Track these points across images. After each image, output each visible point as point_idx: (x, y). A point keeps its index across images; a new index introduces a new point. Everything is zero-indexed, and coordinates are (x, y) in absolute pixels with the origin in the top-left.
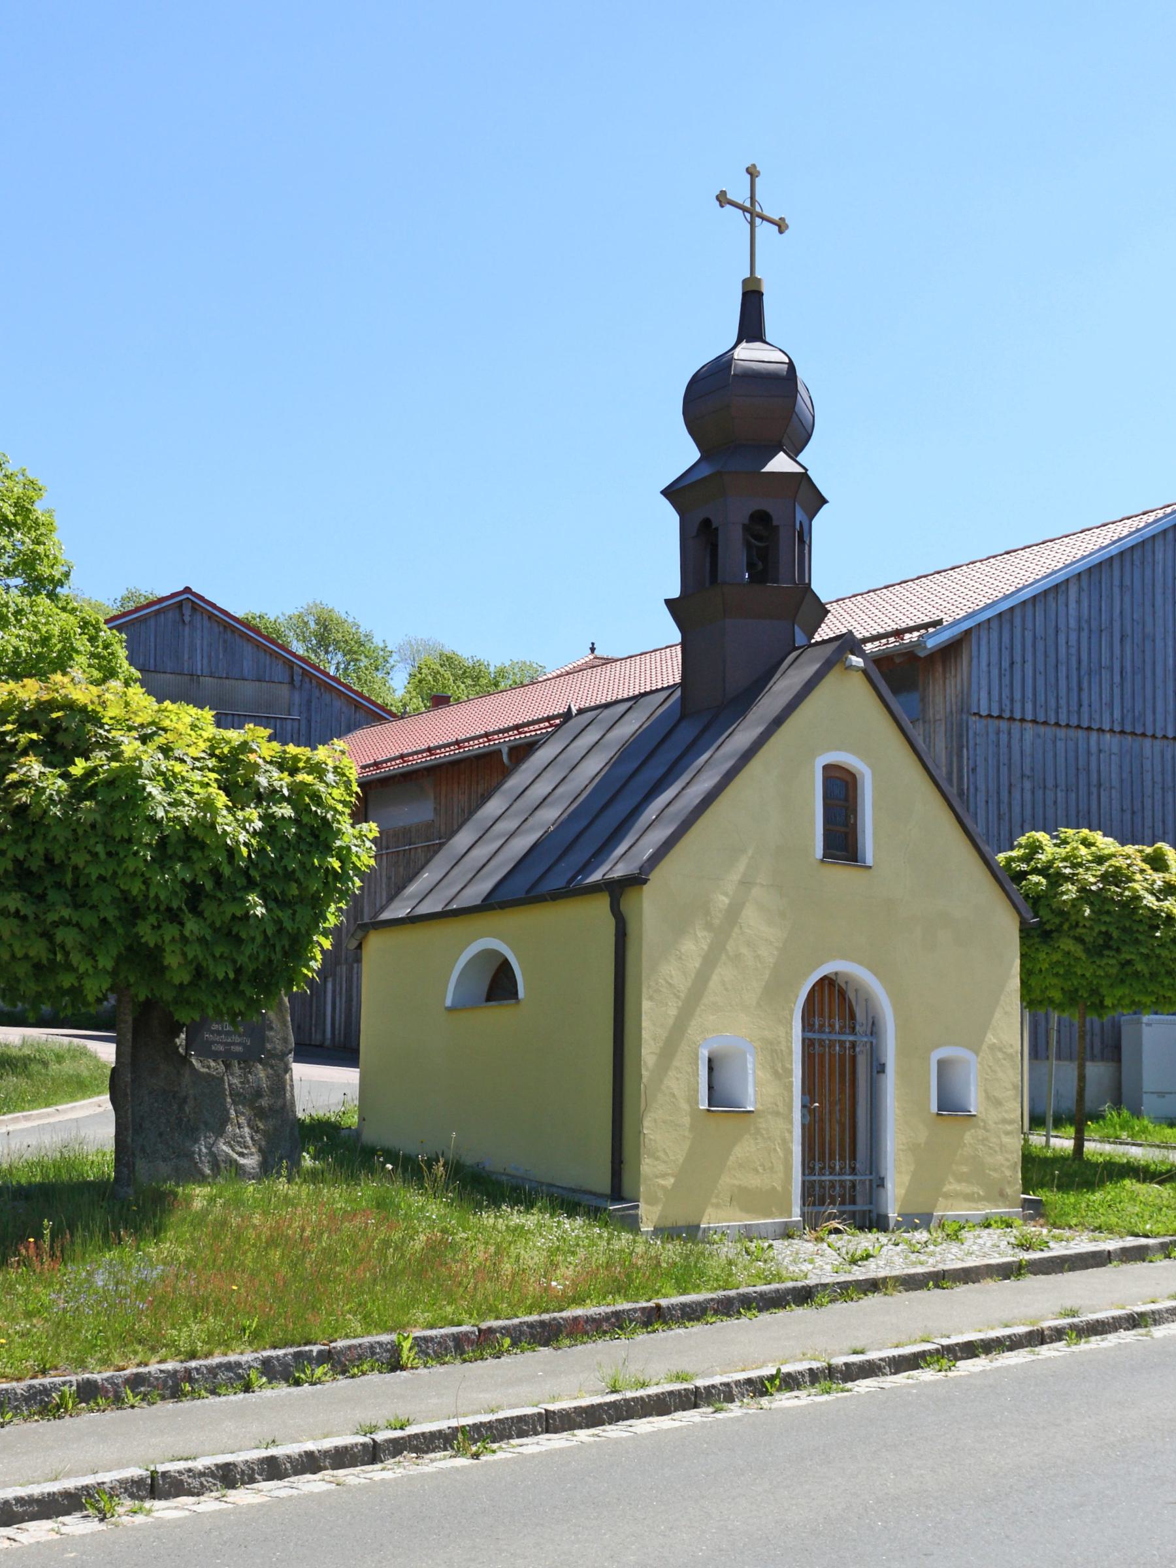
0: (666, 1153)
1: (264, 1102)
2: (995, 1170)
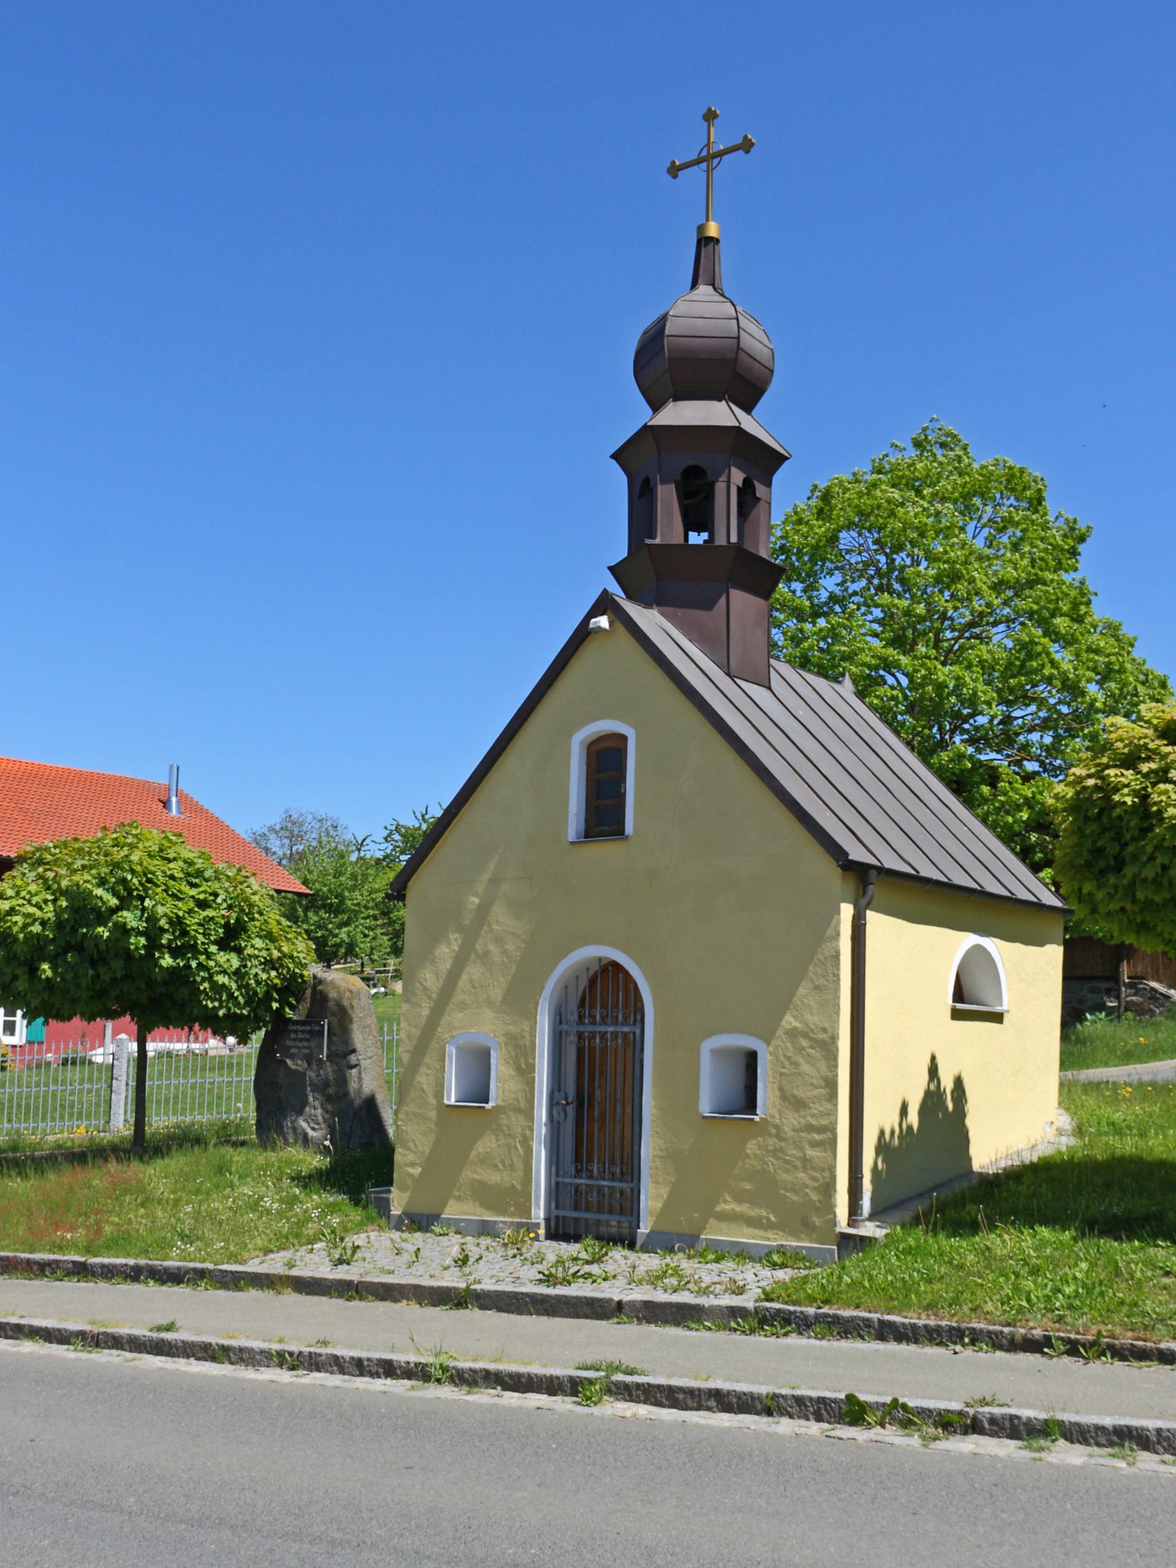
0: (415, 1145)
1: (331, 1090)
2: (794, 1191)
